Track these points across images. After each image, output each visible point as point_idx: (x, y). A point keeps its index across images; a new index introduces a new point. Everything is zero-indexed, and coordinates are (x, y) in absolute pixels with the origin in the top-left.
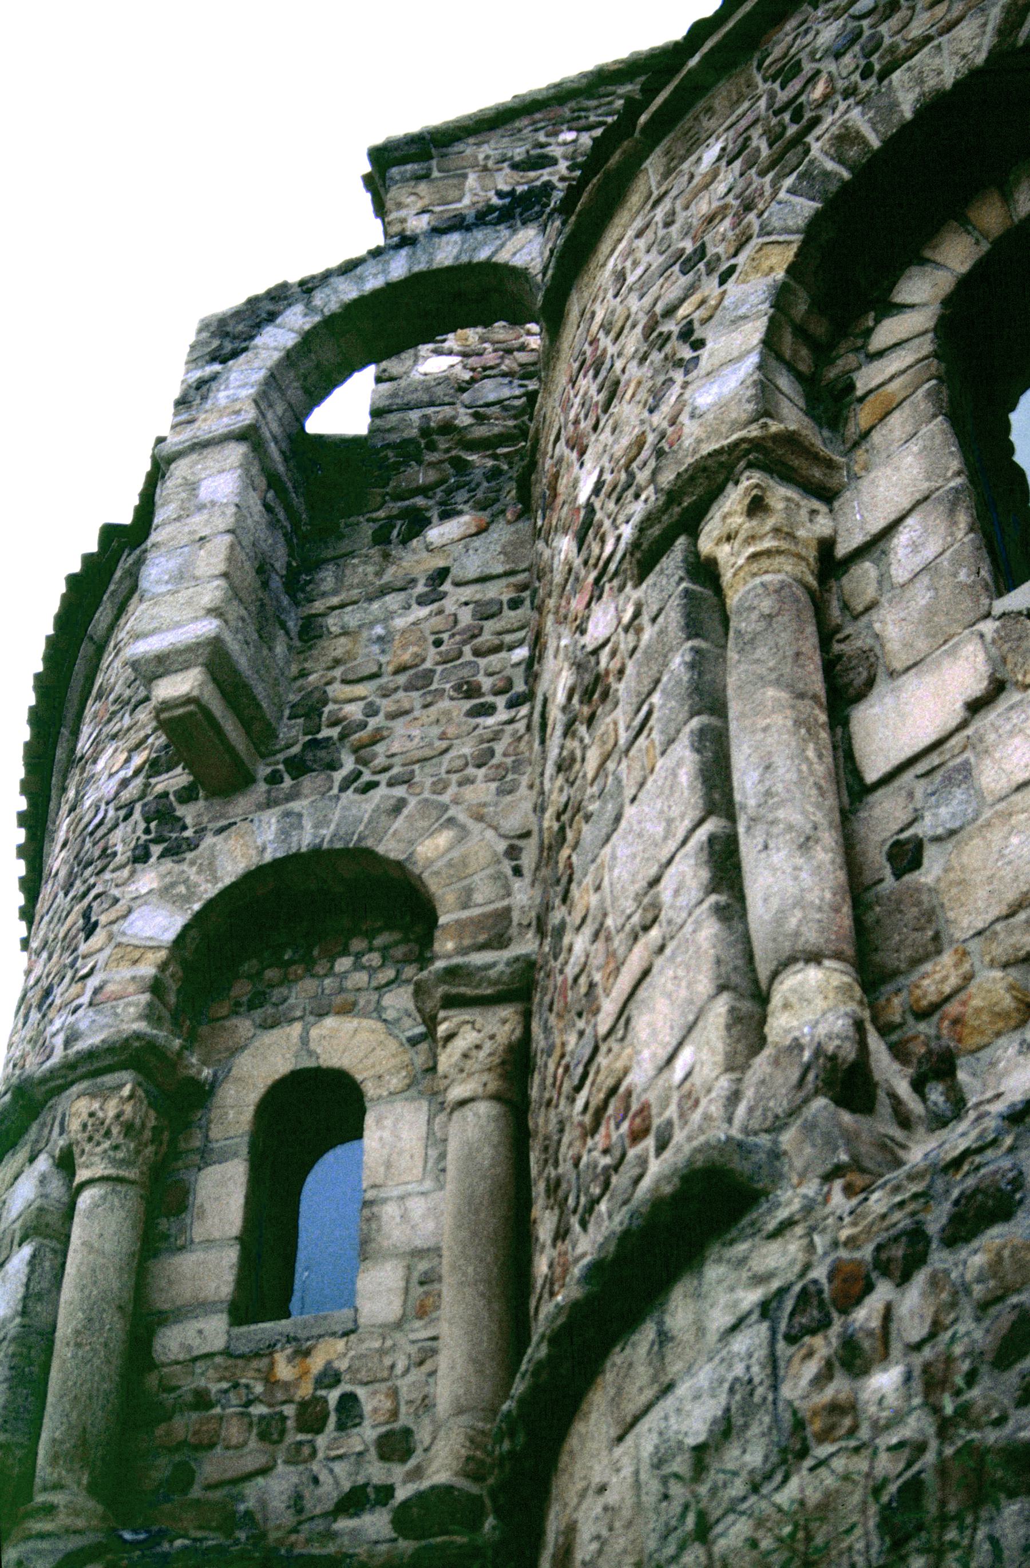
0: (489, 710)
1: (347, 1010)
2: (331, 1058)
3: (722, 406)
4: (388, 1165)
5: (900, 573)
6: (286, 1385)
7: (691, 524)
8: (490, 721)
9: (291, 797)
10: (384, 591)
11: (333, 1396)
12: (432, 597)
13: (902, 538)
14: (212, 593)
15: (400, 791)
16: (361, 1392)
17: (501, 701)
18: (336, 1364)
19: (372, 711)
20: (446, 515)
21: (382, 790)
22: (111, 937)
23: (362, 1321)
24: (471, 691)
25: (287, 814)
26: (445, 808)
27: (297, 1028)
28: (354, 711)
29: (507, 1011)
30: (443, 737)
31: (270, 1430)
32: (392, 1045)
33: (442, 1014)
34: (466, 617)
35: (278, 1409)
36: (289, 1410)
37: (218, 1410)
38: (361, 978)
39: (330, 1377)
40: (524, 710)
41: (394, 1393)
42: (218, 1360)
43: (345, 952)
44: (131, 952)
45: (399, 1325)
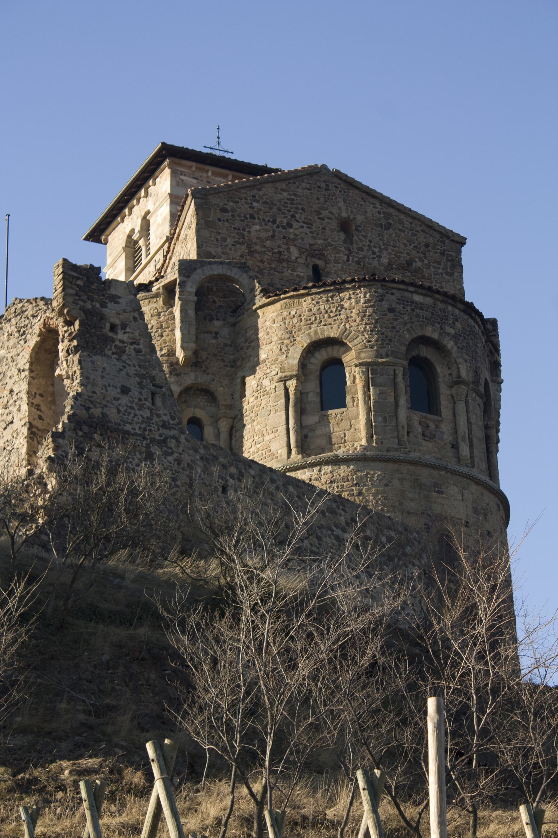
0: (226, 366)
3: (293, 366)
5: (310, 399)
7: (285, 381)
8: (228, 369)
10: (208, 332)
12: (216, 338)
13: (311, 395)
14: (194, 338)
15: (213, 377)
17: (229, 365)
19: (207, 358)
20: (217, 319)
24: (224, 361)
28: (204, 357)
29: (231, 420)
34: (222, 345)
38: (202, 403)
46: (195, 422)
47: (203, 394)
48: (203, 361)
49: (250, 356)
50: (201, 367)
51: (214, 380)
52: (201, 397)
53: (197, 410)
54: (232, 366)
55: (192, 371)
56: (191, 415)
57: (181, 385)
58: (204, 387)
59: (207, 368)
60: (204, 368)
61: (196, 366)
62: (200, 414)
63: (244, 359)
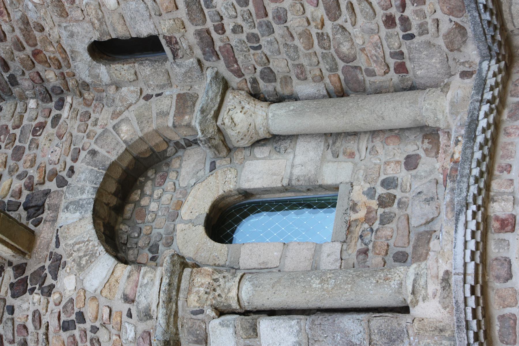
0: (57, 118)
1: (180, 204)
2: (204, 208)
4: (274, 174)
6: (368, 213)
9: (56, 209)
11: (380, 191)
15: (83, 154)
16: (383, 177)
17: (55, 112)
18: (365, 189)
21: (77, 166)
22: (94, 298)
23: (348, 180)
25: (67, 208)
26: (105, 131)
27: (180, 227)
28: (18, 184)
29: (229, 95)
30: (60, 137)
31: (385, 220)
32: (211, 179)
33: (219, 123)
35: (378, 216)
36: (381, 211)
37: (370, 246)
38: (166, 198)
39: (370, 193)
40: (69, 99)
41: (387, 163)
42: (345, 247)
43: (147, 207)
44: (109, 283)
45: (355, 164)
46: (222, 222)
47: (135, 196)
48: (30, 187)
49: (25, 21)
50: (47, 193)
51: (93, 153)
52: (144, 202)
53: (185, 212)
54: (60, 105)
55: (54, 220)
56: (201, 230)
57: (92, 256)
58: (113, 187)
59: (54, 174)
60: (52, 185)
61: (40, 208)
62: (198, 203)
63: (36, 53)
